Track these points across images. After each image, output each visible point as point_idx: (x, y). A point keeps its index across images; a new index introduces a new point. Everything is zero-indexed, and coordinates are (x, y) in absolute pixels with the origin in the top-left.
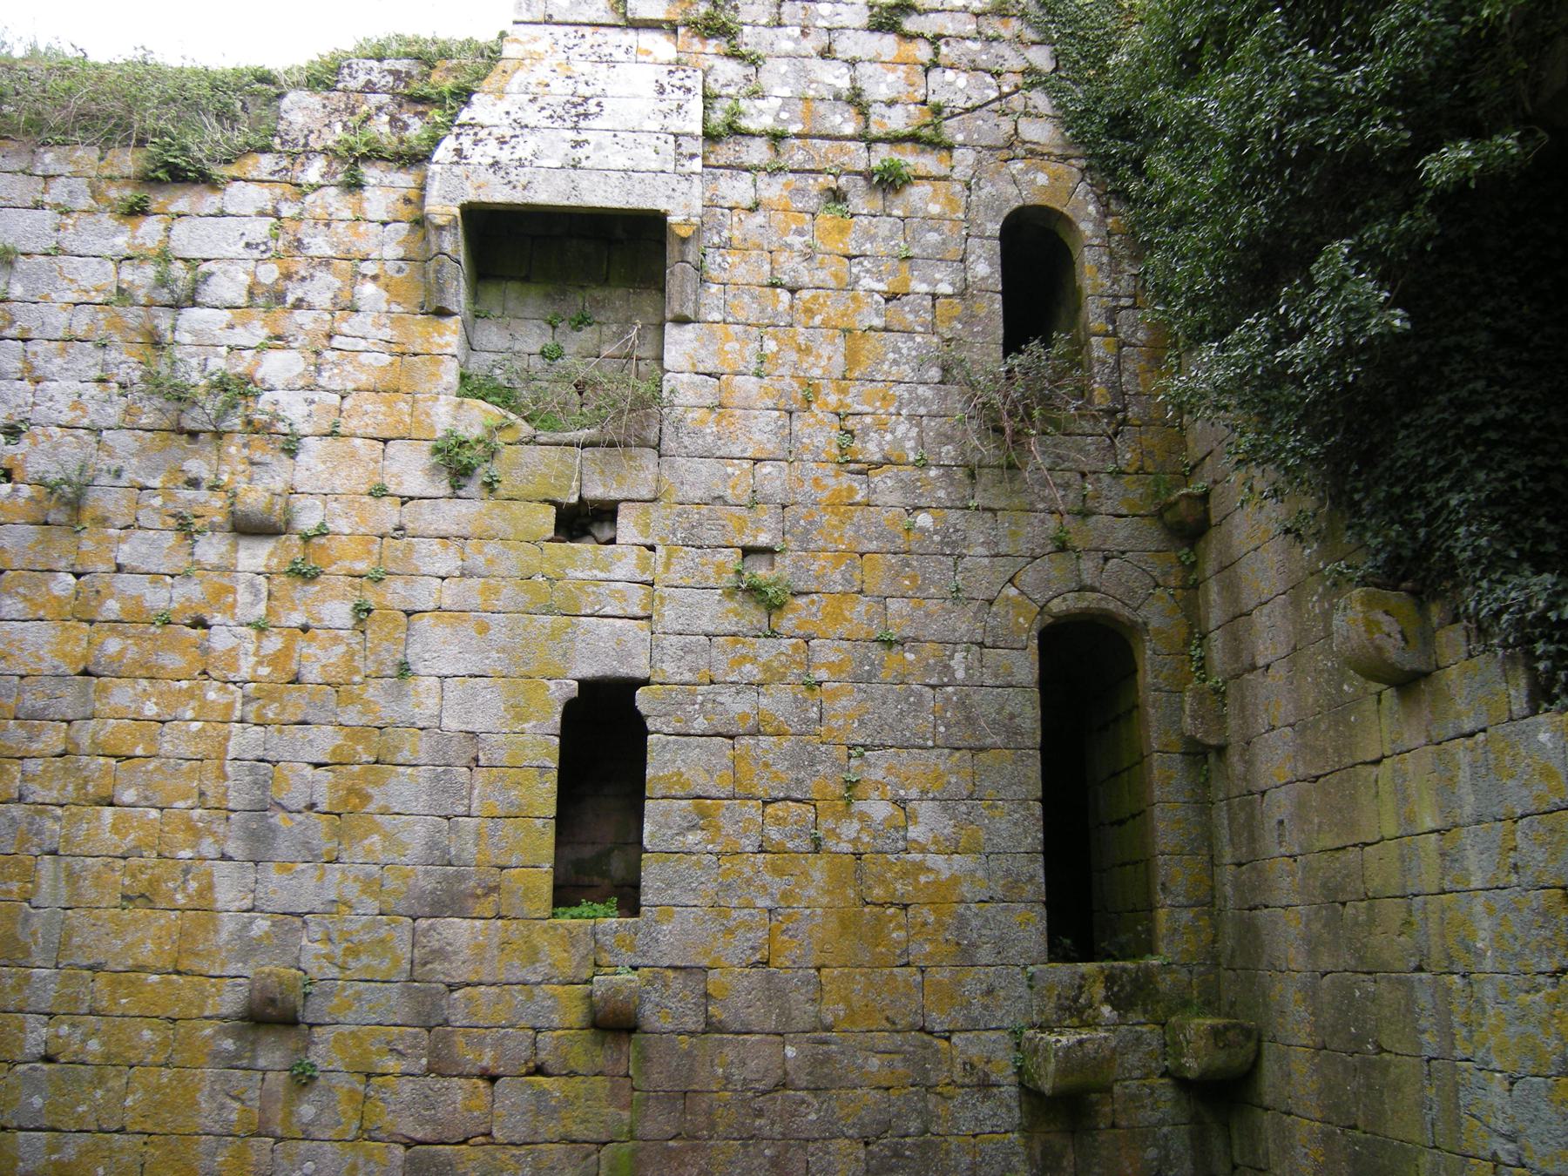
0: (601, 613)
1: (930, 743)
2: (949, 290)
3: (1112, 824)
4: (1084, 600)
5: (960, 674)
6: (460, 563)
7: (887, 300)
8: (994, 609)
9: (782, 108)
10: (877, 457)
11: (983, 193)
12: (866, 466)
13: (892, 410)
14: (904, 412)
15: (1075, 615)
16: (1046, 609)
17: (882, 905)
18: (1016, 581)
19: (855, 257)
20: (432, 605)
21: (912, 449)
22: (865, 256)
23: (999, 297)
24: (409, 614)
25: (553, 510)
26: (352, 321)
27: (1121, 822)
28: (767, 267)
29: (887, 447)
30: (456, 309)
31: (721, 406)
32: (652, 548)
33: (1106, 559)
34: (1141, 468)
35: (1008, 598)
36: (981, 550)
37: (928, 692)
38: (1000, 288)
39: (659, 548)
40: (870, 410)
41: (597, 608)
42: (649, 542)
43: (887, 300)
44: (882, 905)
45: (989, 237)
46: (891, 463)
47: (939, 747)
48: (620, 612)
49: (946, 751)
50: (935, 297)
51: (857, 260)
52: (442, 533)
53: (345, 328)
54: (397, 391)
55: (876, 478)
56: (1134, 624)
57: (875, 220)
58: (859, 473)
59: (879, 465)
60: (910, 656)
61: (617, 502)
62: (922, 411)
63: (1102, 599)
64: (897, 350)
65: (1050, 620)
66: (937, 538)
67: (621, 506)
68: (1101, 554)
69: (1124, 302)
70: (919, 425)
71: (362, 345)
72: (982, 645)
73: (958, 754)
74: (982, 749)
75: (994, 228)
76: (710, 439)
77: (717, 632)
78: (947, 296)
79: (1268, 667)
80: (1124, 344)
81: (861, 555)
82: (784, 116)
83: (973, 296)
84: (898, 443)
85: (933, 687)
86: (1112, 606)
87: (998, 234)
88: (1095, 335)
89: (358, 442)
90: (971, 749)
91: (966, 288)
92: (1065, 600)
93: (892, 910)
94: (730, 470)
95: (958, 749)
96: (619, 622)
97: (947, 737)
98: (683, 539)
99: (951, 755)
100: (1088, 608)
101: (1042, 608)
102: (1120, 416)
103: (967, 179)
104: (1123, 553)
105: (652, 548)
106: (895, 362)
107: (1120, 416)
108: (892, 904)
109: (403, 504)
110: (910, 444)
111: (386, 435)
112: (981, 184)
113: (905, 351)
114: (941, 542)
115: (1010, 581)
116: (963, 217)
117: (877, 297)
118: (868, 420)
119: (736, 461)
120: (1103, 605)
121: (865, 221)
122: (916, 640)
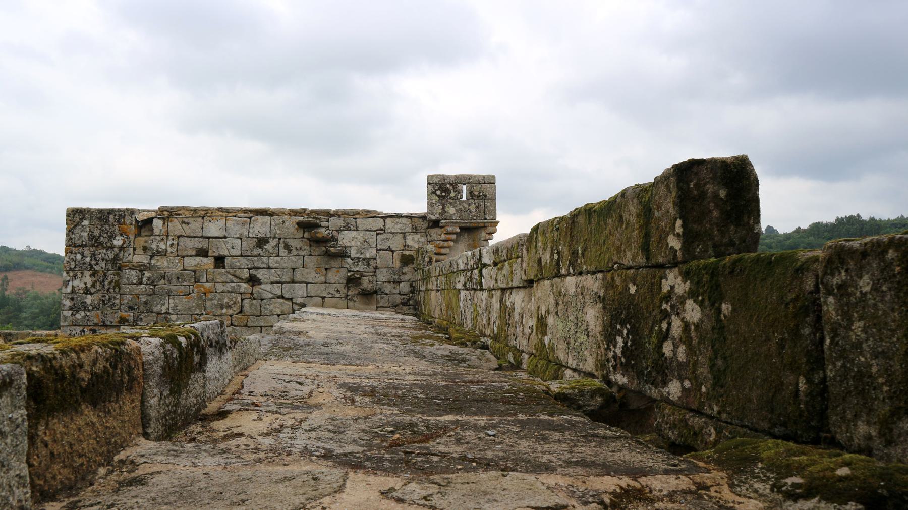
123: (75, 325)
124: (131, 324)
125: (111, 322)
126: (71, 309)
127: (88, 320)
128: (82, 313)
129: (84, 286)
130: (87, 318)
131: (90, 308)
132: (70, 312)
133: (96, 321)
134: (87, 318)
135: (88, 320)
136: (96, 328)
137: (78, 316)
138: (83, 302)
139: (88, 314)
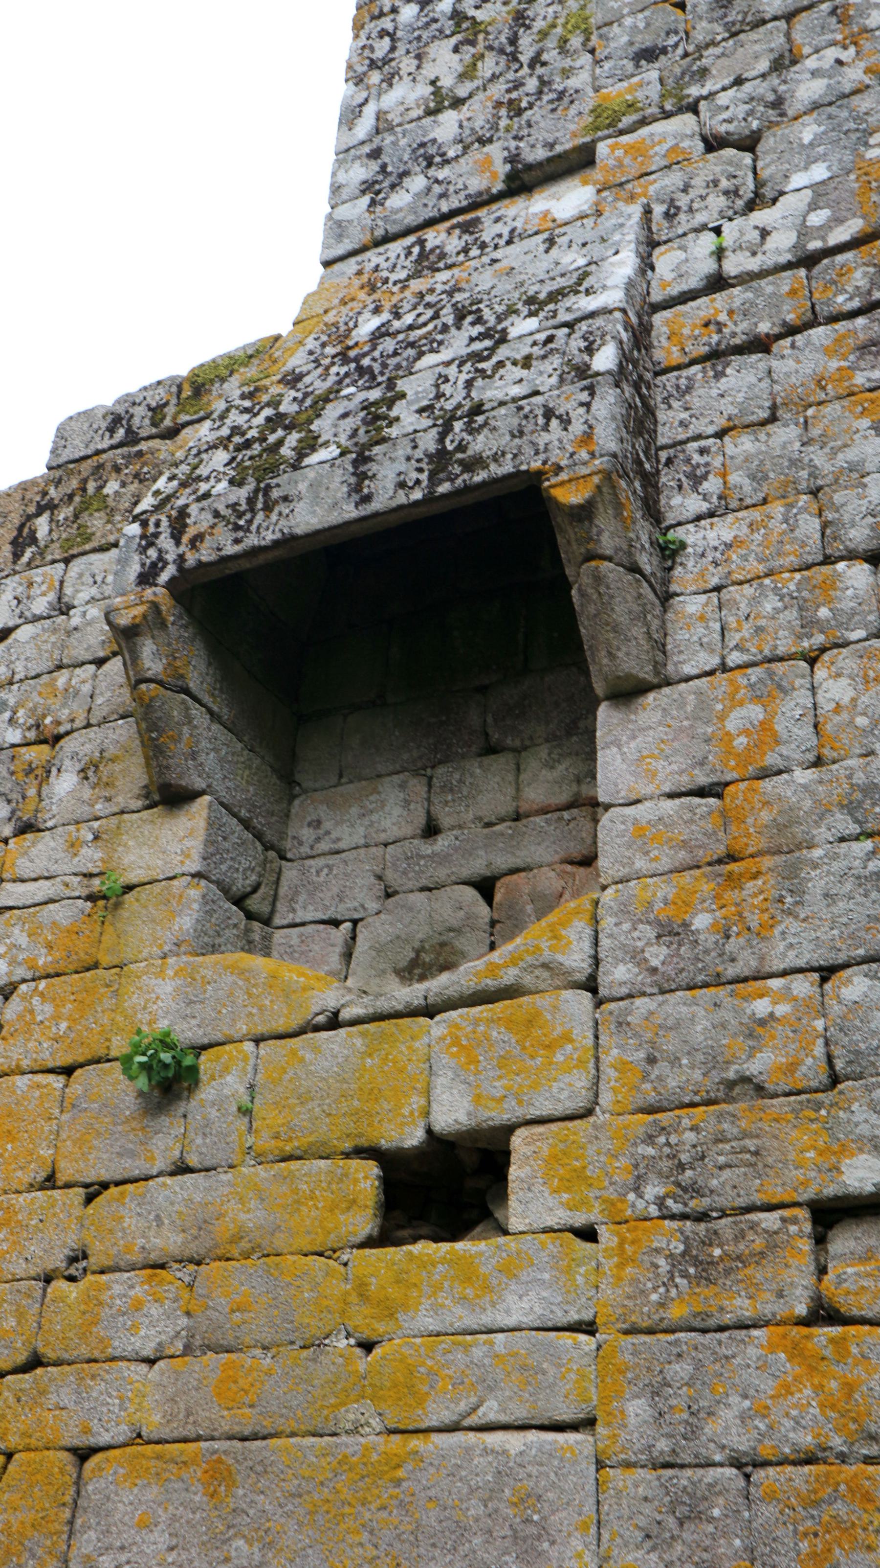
0: (473, 1420)
6: (184, 1321)
9: (813, 206)
20: (122, 1432)
24: (83, 1454)
25: (372, 1169)
26: (34, 851)
28: (810, 526)
30: (199, 784)
31: (731, 857)
32: (588, 1234)
39: (603, 1232)
41: (463, 1406)
42: (579, 1219)
48: (519, 1413)
52: (153, 1257)
53: (24, 867)
54: (96, 966)
61: (509, 1129)
67: (517, 1140)
71: (42, 889)
76: (708, 940)
77: (765, 1452)
82: (817, 218)
89: (22, 1082)
94: (761, 1007)
96: (514, 1441)
98: (660, 1202)
105: (588, 1234)
109: (89, 1199)
111: (64, 1059)
119: (775, 983)
123: (387, 239)
124: (654, 110)
125: (552, 146)
126: (367, 187)
127: (442, 196)
128: (417, 183)
129: (431, 89)
130: (437, 189)
131: (451, 154)
132: (366, 200)
133: (476, 184)
134: (437, 189)
135: (442, 196)
136: (482, 213)
137: (398, 200)
138: (423, 145)
139: (441, 174)
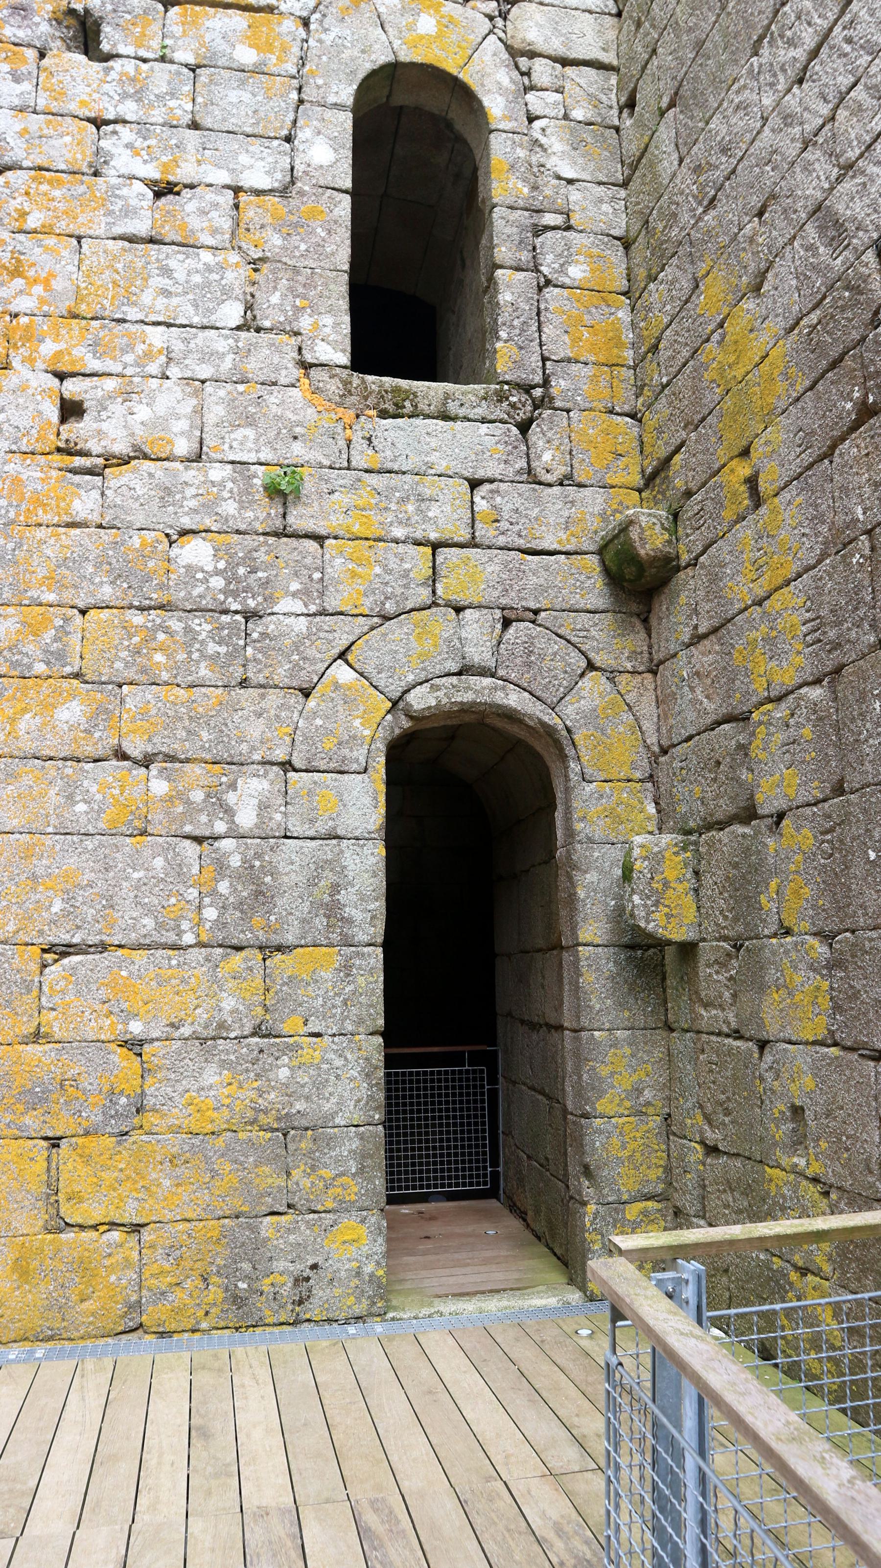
1: (189, 938)
2: (264, 182)
3: (523, 1022)
4: (468, 688)
5: (246, 819)
7: (158, 195)
8: (312, 703)
10: (121, 447)
11: (328, 38)
12: (101, 461)
13: (153, 368)
14: (174, 372)
15: (449, 714)
16: (401, 705)
17: (95, 1227)
18: (350, 657)
19: (107, 122)
21: (182, 433)
22: (125, 122)
23: (347, 200)
27: (534, 1026)
29: (139, 431)
33: (507, 623)
34: (569, 477)
35: (337, 686)
36: (298, 606)
37: (190, 849)
38: (348, 184)
40: (117, 368)
43: (158, 195)
44: (95, 1227)
45: (335, 105)
46: (146, 457)
47: (205, 946)
49: (219, 951)
50: (237, 190)
51: (110, 128)
55: (117, 478)
56: (549, 731)
57: (145, 67)
58: (90, 472)
59: (125, 461)
60: (160, 787)
62: (205, 371)
63: (496, 689)
64: (166, 272)
65: (406, 724)
66: (217, 582)
68: (498, 614)
69: (550, 219)
70: (196, 393)
72: (287, 766)
73: (237, 959)
74: (279, 948)
75: (346, 93)
78: (259, 193)
79: (781, 816)
80: (548, 282)
81: (83, 612)
83: (301, 193)
84: (160, 423)
85: (198, 840)
86: (514, 699)
87: (350, 101)
88: (501, 267)
90: (261, 948)
91: (293, 183)
92: (437, 688)
93: (116, 1235)
95: (239, 948)
97: (221, 924)
99: (225, 956)
100: (474, 703)
101: (395, 703)
102: (538, 392)
103: (305, 14)
104: (536, 612)
106: (165, 293)
107: (538, 392)
108: (113, 1225)
110: (182, 425)
112: (327, 21)
113: (181, 276)
114: (225, 592)
115: (342, 655)
116: (293, 71)
117: (139, 187)
118: (110, 384)
120: (499, 698)
121: (130, 66)
122: (171, 758)
